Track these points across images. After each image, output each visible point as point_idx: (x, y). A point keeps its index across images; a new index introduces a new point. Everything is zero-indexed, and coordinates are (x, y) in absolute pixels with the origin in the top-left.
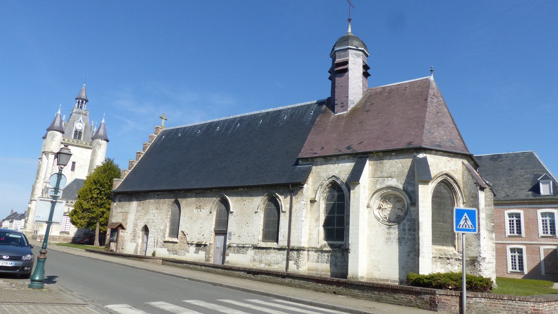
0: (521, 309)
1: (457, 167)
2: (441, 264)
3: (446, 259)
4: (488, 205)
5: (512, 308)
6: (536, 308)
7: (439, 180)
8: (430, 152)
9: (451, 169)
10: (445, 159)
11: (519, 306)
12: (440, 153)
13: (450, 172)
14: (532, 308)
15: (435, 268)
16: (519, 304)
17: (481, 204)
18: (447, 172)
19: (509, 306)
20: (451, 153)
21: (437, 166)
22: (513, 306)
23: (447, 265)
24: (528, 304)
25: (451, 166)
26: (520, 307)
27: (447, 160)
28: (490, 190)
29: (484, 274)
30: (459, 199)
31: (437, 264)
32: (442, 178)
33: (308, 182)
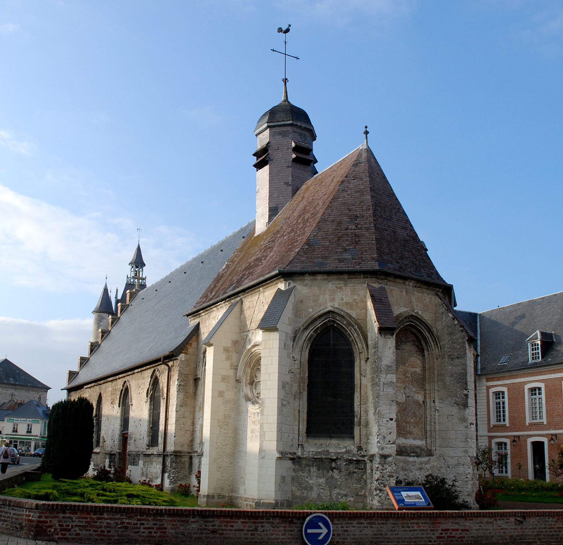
0: (16, 519)
1: (356, 297)
2: (319, 470)
3: (328, 460)
4: (457, 357)
5: (7, 518)
6: (30, 518)
7: (319, 324)
8: (302, 278)
9: (345, 301)
10: (331, 285)
11: (14, 514)
12: (319, 277)
13: (341, 307)
14: (27, 518)
15: (307, 478)
16: (14, 512)
17: (383, 359)
18: (334, 308)
19: (5, 515)
20: (341, 273)
21: (315, 301)
22: (8, 515)
23: (330, 471)
24: (23, 511)
25: (344, 297)
26: (15, 516)
27: (336, 287)
28: (461, 329)
29: (384, 486)
30: (360, 352)
31: (311, 469)
32: (326, 319)
33: (189, 350)
